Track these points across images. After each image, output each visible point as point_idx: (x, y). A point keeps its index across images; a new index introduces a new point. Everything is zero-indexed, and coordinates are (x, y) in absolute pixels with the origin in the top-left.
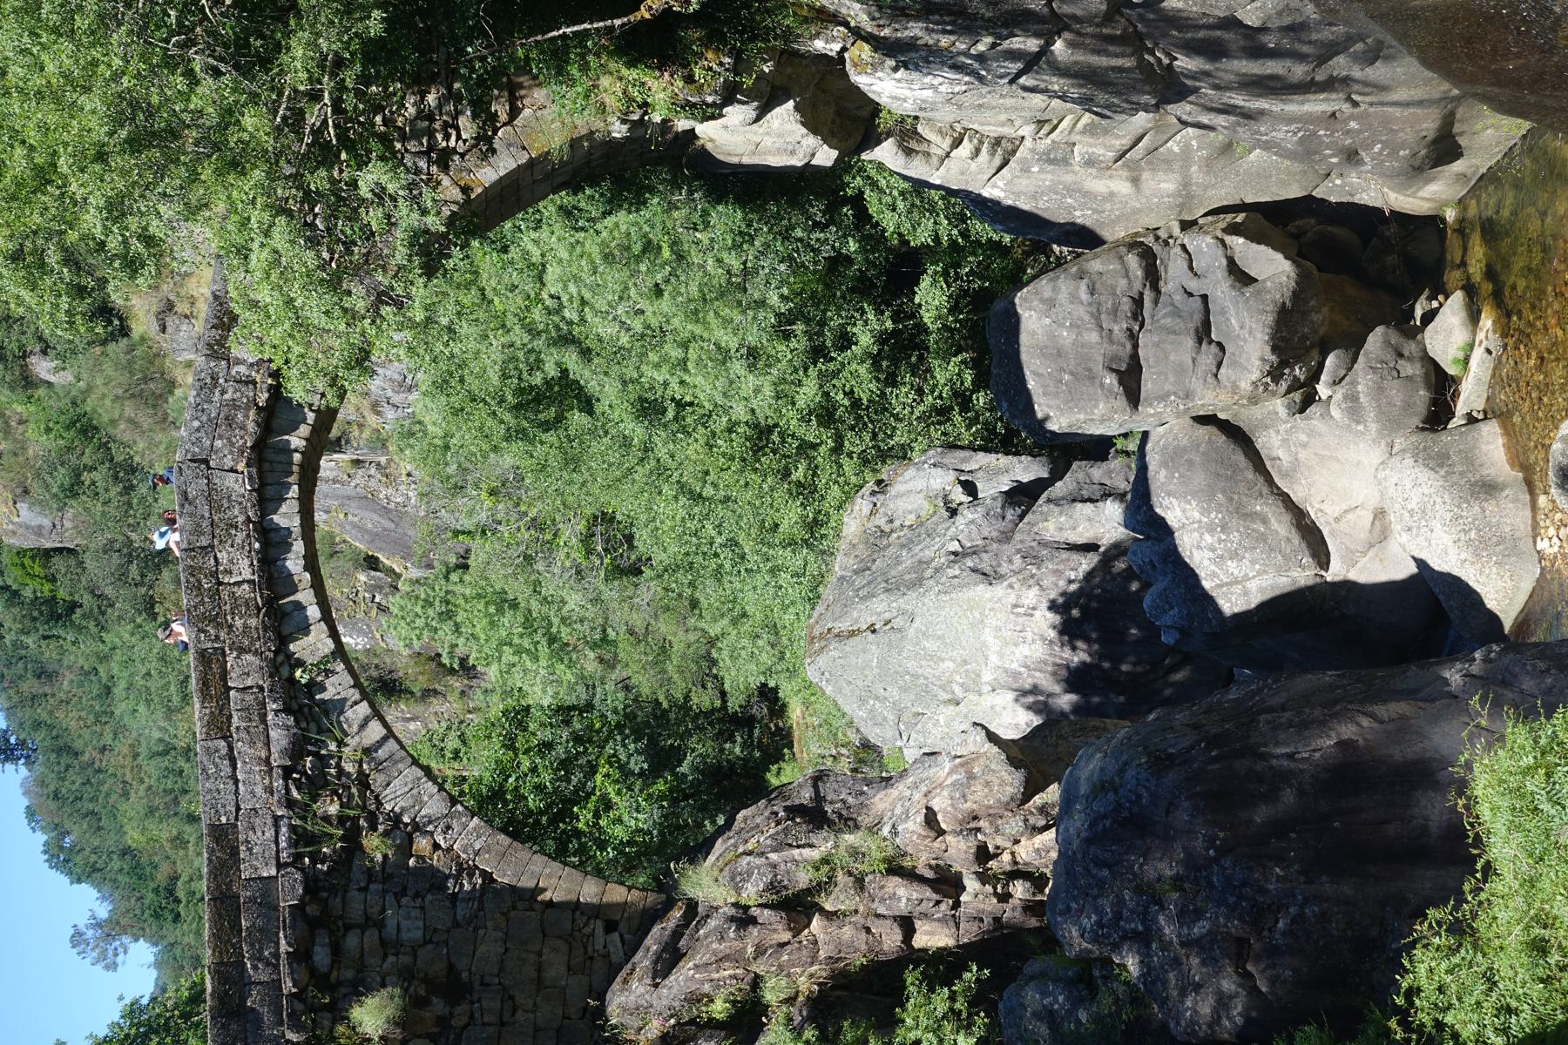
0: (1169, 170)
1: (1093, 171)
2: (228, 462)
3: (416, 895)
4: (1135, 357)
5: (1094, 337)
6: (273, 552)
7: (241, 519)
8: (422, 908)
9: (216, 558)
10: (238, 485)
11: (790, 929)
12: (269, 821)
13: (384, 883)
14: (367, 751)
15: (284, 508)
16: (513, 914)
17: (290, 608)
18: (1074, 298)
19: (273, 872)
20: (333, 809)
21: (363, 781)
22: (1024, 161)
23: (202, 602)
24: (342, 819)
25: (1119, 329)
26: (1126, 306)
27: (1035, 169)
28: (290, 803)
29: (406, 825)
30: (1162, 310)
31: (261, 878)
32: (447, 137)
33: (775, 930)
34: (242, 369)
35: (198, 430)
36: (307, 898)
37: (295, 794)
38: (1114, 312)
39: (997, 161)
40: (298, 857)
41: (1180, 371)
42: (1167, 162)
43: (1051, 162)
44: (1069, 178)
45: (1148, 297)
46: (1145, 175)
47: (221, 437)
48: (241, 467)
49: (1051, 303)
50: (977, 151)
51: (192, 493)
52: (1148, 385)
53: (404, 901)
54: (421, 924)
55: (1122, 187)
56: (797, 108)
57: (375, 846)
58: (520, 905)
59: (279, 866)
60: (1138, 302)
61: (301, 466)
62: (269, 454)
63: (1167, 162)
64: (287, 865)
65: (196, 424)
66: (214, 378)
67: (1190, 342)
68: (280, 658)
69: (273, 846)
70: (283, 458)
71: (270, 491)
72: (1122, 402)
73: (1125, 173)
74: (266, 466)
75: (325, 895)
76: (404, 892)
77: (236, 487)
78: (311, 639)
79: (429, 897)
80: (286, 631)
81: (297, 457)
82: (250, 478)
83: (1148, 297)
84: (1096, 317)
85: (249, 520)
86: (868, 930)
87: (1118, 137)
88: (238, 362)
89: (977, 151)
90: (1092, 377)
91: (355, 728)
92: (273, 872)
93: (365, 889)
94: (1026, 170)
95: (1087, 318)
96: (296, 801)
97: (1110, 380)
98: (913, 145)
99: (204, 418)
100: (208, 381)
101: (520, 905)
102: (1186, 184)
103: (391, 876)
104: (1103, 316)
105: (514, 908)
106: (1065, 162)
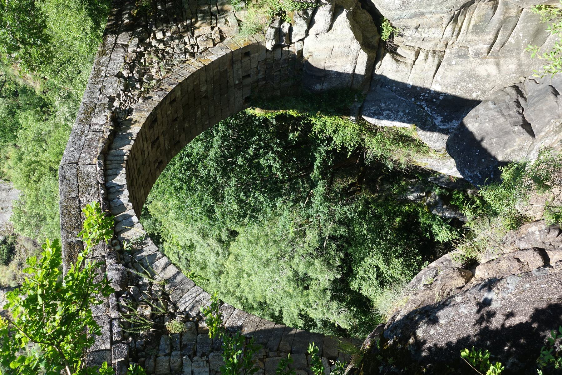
0: (511, 56)
1: (479, 60)
2: (88, 161)
3: (203, 355)
4: (524, 120)
5: (502, 120)
6: (111, 196)
7: (94, 183)
8: (208, 361)
9: (79, 201)
10: (92, 168)
11: (463, 276)
12: (107, 321)
13: (181, 350)
14: (168, 281)
15: (118, 178)
16: (267, 360)
17: (120, 219)
18: (487, 109)
19: (108, 346)
20: (147, 312)
21: (165, 296)
22: (448, 59)
23: (71, 220)
24: (152, 316)
25: (513, 111)
26: (513, 104)
27: (453, 63)
28: (119, 308)
29: (194, 318)
30: (530, 101)
31: (100, 351)
32: (193, 48)
33: (452, 278)
34: (97, 127)
35: (73, 151)
36: (130, 359)
37: (123, 303)
38: (508, 108)
39: (436, 62)
40: (124, 337)
41: (551, 109)
42: (510, 51)
43: (460, 57)
44: (469, 67)
45: (521, 100)
46: (502, 61)
47: (85, 152)
48: (95, 160)
49: (476, 117)
50: (427, 56)
51: (68, 175)
52: (535, 127)
53: (195, 358)
54: (207, 369)
55: (492, 69)
56: (348, 15)
57: (174, 326)
58: (271, 354)
59: (112, 343)
60: (518, 104)
61: (127, 161)
62: (110, 157)
63: (510, 51)
64: (117, 342)
65: (72, 149)
66: (83, 132)
67: (552, 97)
68: (114, 241)
69: (109, 333)
70: (117, 158)
71: (110, 172)
72: (526, 135)
73: (493, 60)
74: (108, 162)
75: (143, 359)
76: (195, 354)
77: (92, 170)
78: (133, 230)
79: (212, 354)
80: (118, 229)
81: (125, 157)
82: (100, 164)
83: (521, 100)
84: (500, 112)
85: (98, 183)
86: (518, 260)
87: (488, 33)
88: (95, 124)
89: (427, 56)
90: (507, 133)
91: (160, 270)
92: (108, 346)
93: (169, 354)
94: (449, 64)
95: (496, 114)
96: (124, 307)
97: (517, 128)
98: (398, 58)
99: (76, 146)
100: (79, 132)
101: (271, 354)
102: (520, 65)
103: (186, 346)
104: (503, 111)
105: (267, 357)
106: (465, 56)
